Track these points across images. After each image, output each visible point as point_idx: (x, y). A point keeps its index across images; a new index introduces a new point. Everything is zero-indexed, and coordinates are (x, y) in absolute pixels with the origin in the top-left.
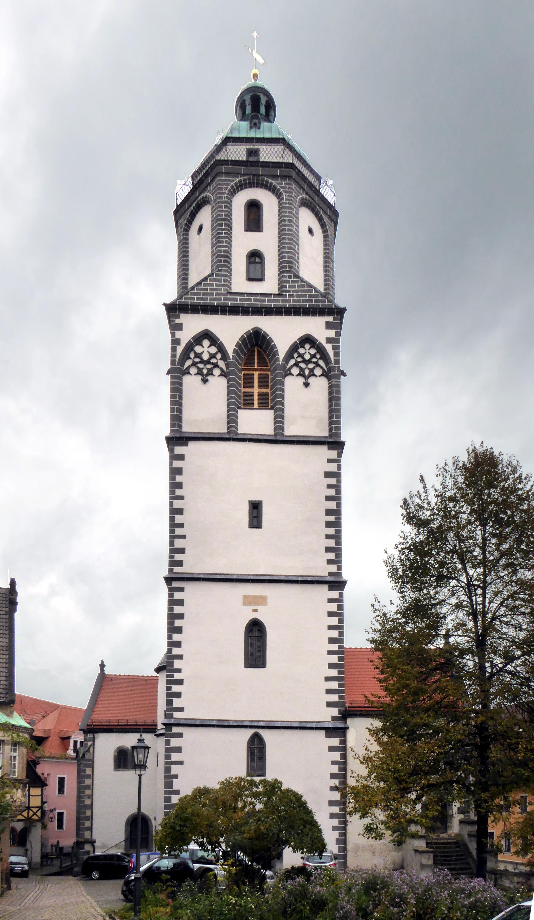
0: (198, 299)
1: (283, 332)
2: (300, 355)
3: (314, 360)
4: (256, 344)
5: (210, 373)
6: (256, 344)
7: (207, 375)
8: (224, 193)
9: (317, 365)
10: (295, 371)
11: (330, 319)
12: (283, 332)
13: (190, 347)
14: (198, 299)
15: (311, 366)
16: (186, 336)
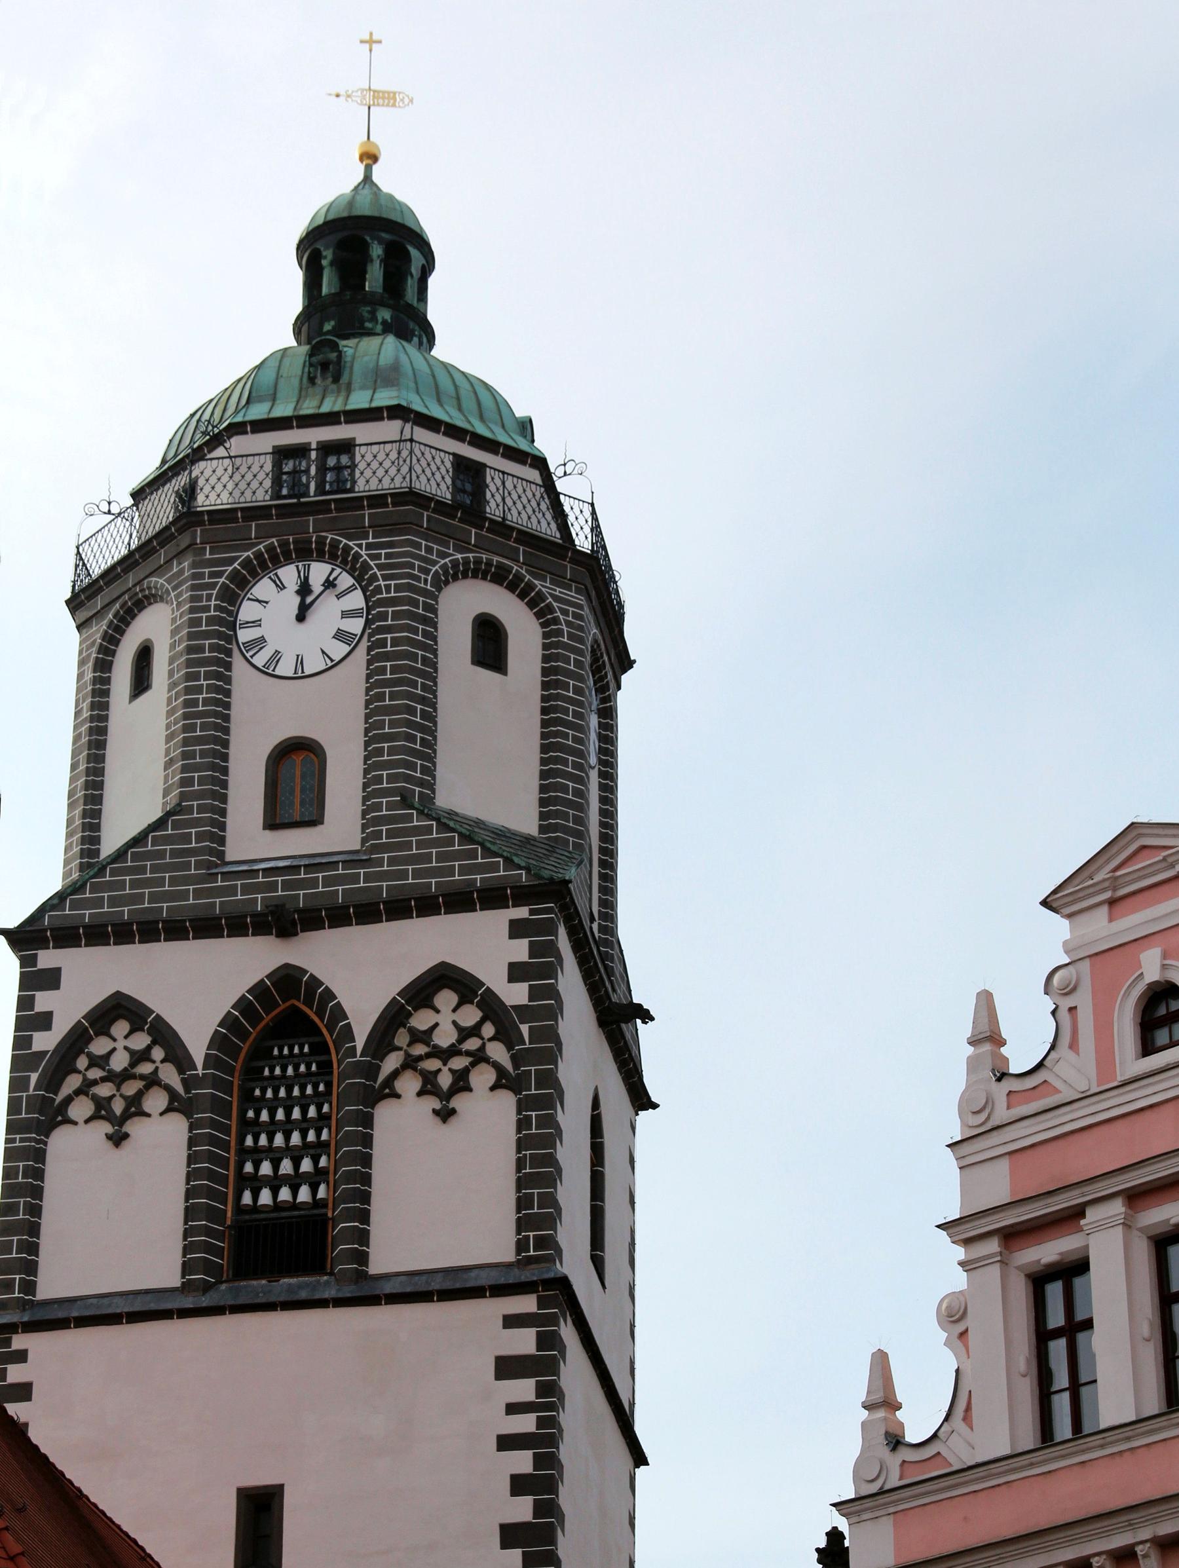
0: (113, 902)
1: (361, 970)
2: (424, 1037)
3: (472, 1044)
4: (286, 1015)
5: (135, 1108)
6: (286, 1015)
7: (126, 1116)
8: (206, 609)
9: (479, 1057)
10: (409, 1084)
11: (522, 912)
12: (361, 970)
13: (77, 1040)
14: (113, 902)
15: (458, 1063)
16: (67, 1007)
